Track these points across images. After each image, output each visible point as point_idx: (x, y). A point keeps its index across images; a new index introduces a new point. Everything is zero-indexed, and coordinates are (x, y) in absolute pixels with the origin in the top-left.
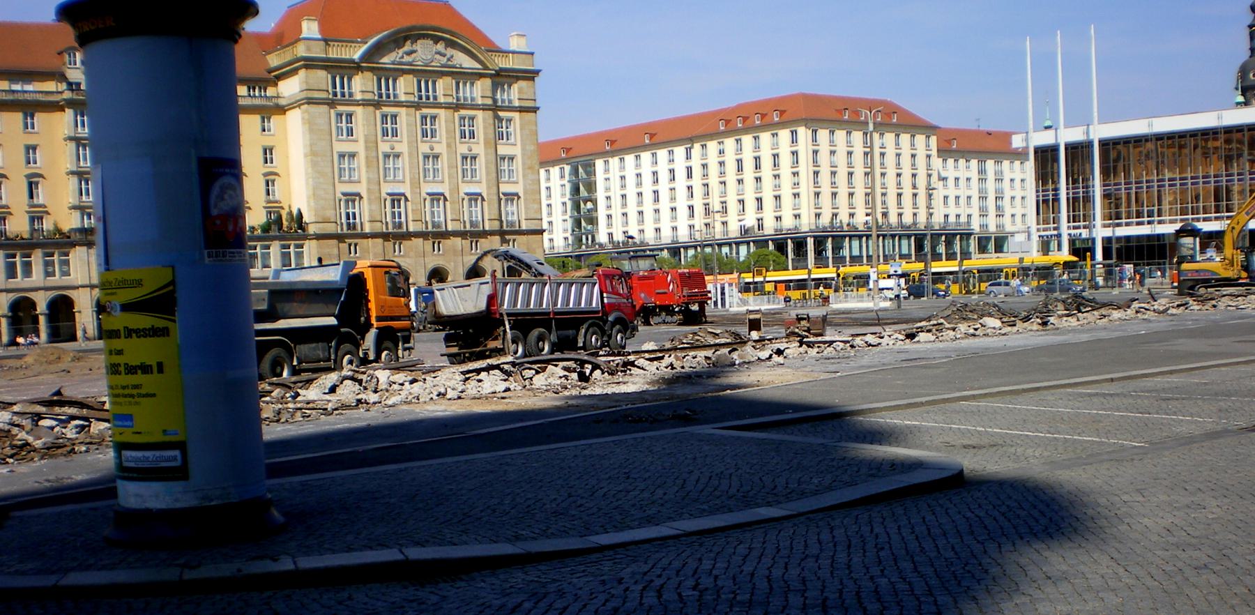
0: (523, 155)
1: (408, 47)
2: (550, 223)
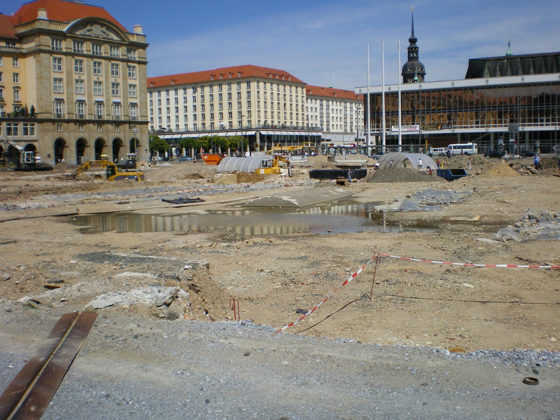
0: (140, 84)
1: (89, 27)
2: (152, 118)
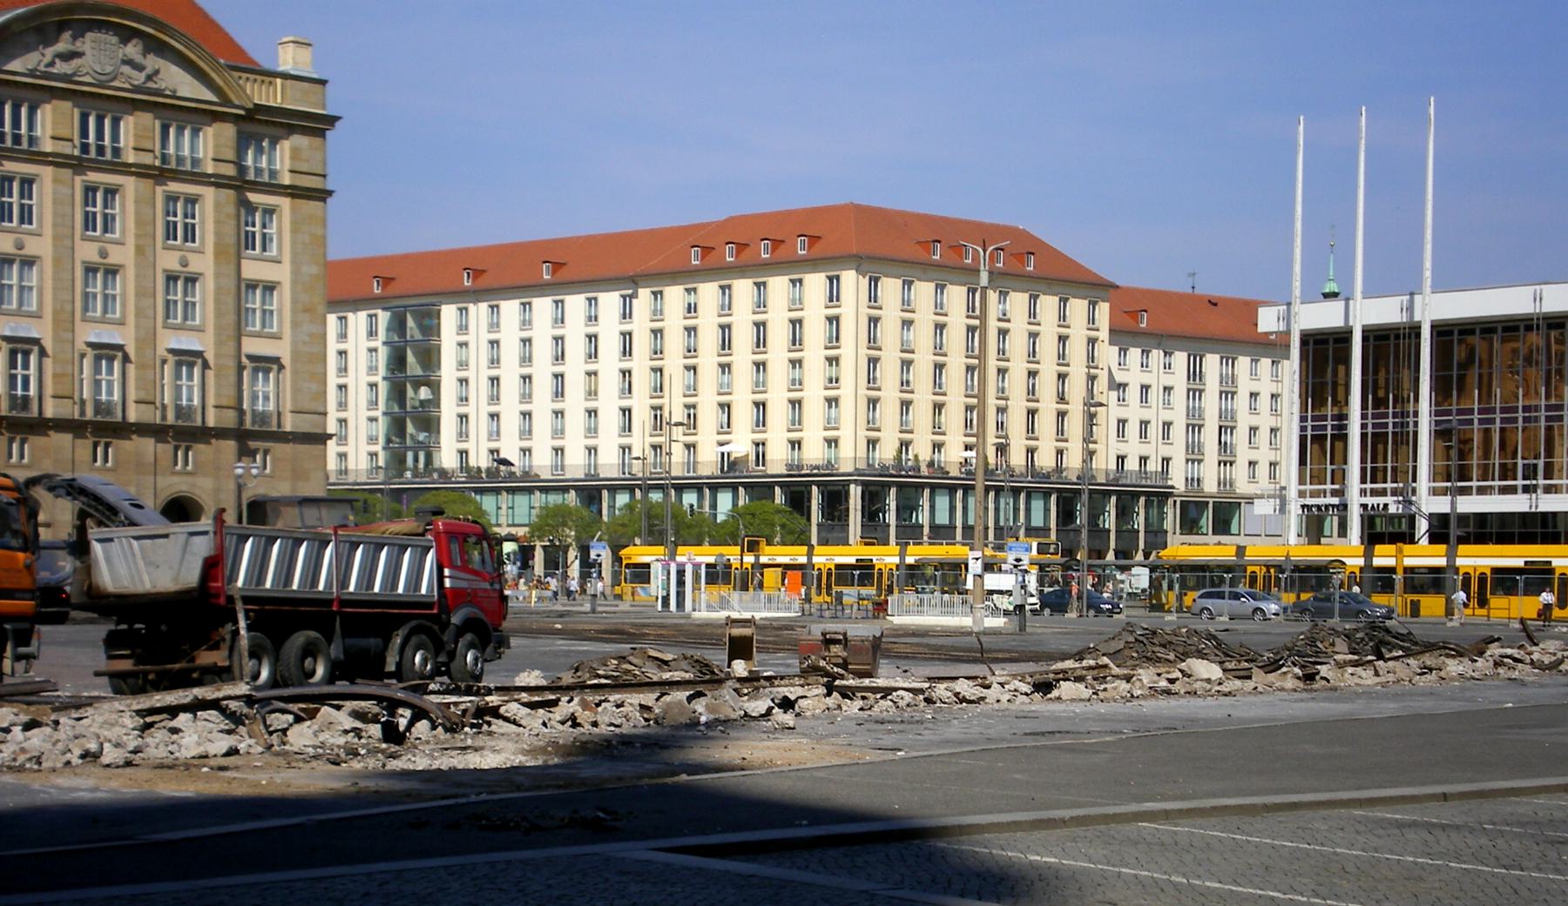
0: (294, 282)
2: (343, 422)
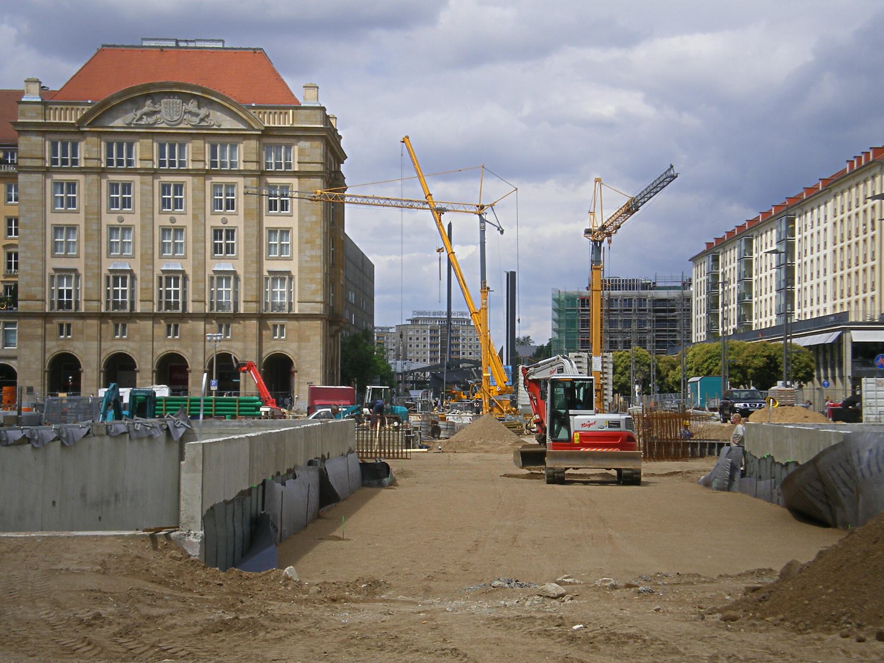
1: (148, 107)
